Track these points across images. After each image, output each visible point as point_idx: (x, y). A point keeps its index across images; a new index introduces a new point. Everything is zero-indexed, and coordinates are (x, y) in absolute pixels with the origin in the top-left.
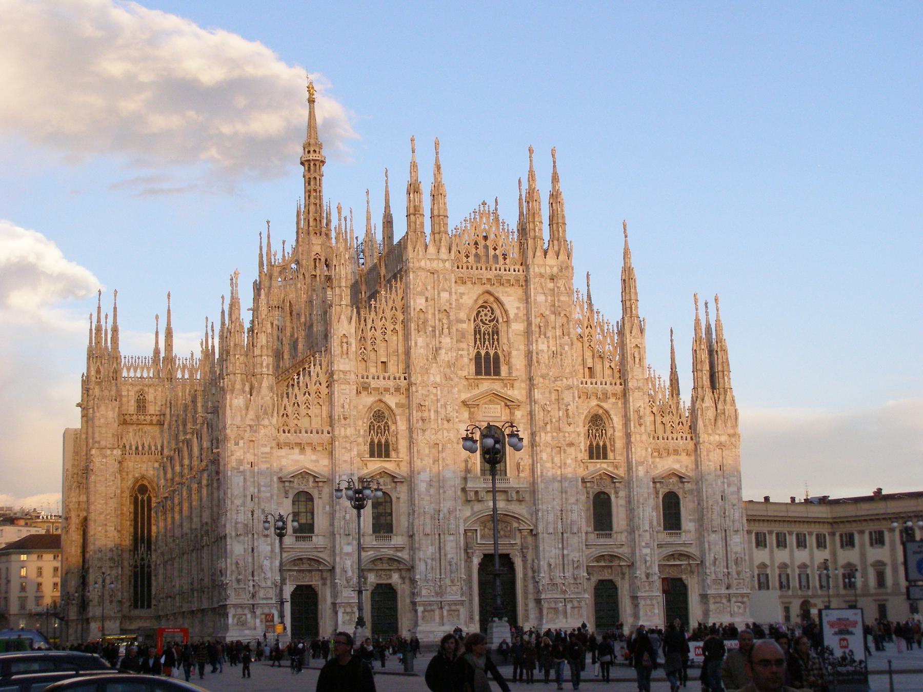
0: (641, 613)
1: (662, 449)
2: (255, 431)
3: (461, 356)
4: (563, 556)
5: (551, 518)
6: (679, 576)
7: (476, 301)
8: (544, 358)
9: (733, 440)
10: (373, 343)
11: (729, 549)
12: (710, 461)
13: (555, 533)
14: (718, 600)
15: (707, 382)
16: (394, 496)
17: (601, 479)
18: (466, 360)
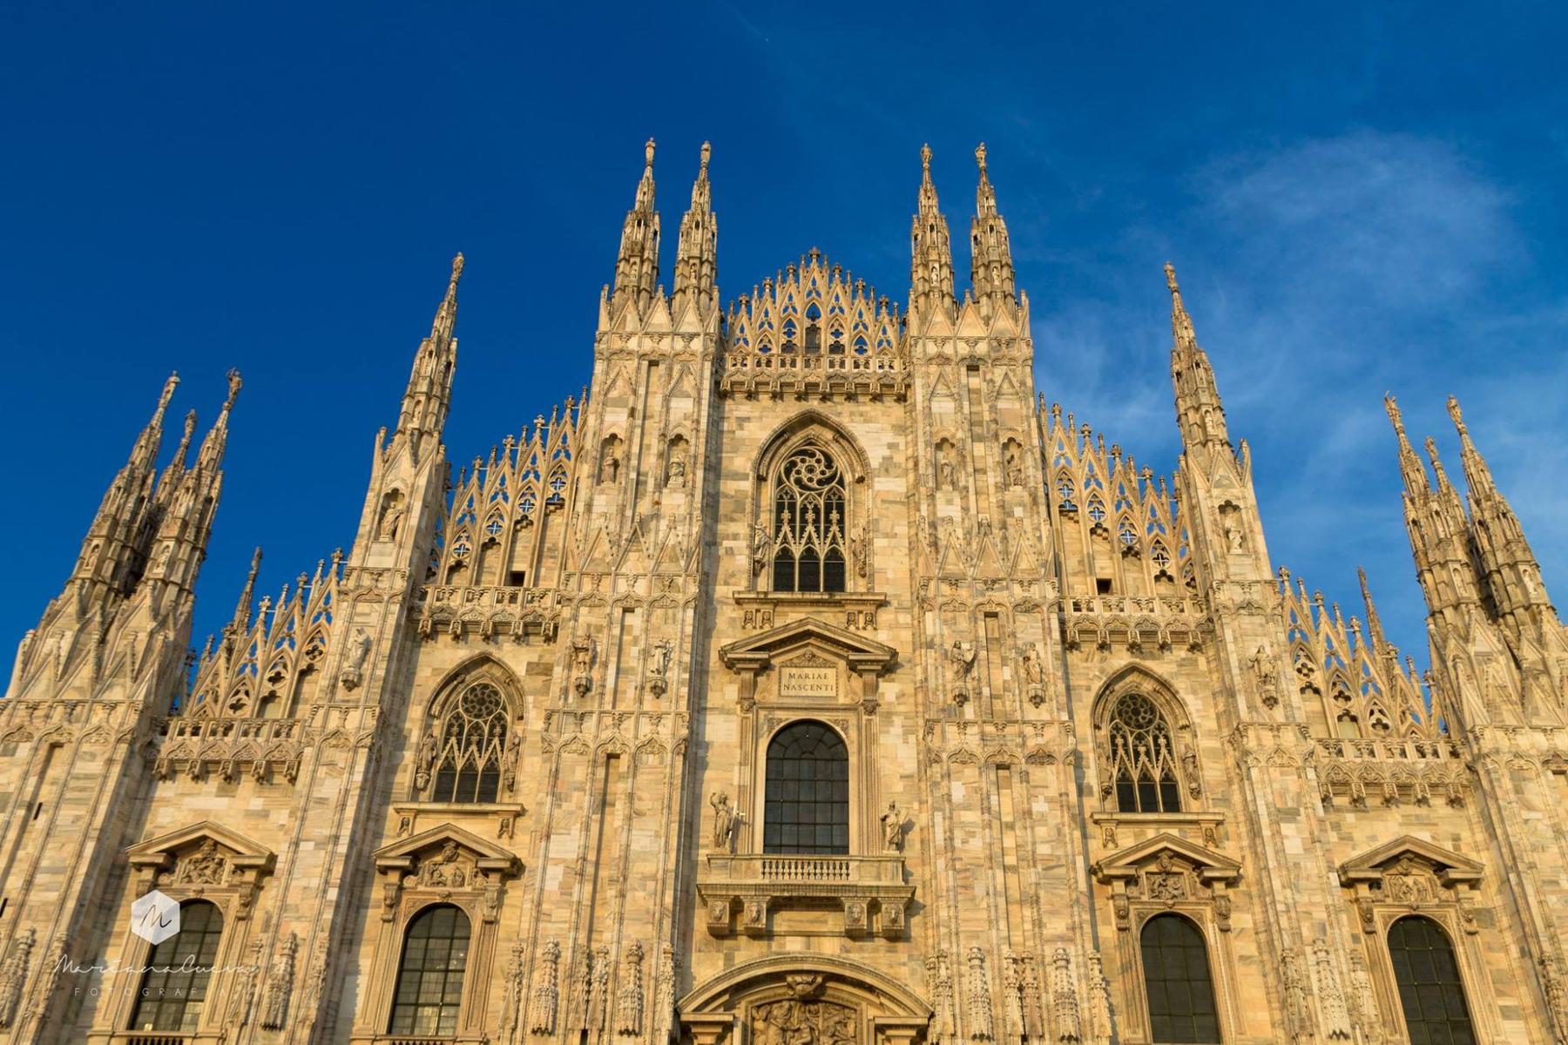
1: (1356, 787)
2: (78, 721)
3: (730, 552)
7: (781, 436)
15: (1472, 594)
16: (478, 915)
18: (743, 561)
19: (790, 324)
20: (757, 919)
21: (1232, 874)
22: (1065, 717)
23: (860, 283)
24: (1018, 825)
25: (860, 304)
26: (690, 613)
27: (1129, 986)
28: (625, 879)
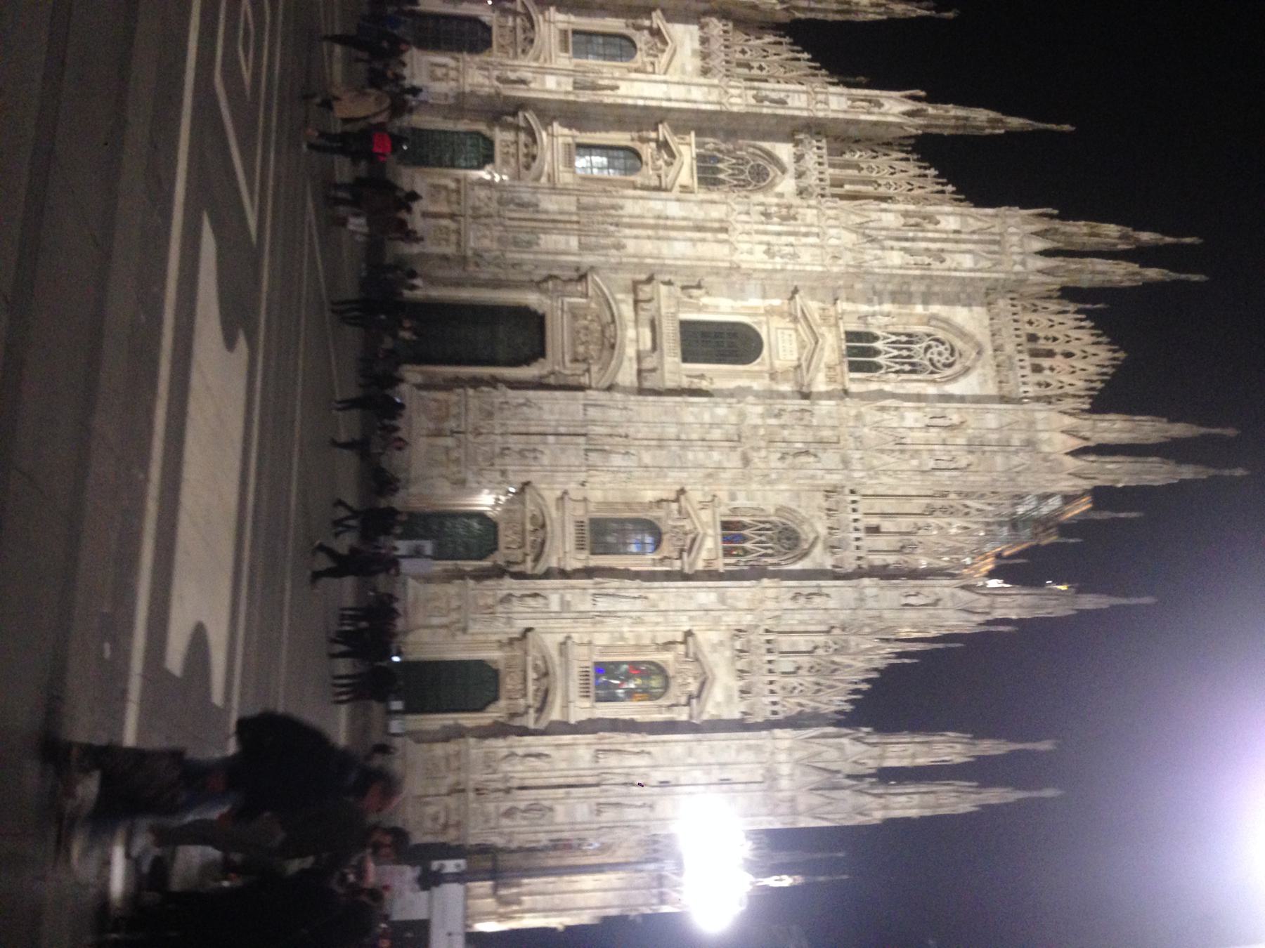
0: (434, 588)
4: (545, 434)
5: (615, 415)
6: (503, 693)
7: (962, 334)
8: (890, 419)
9: (784, 808)
10: (870, 169)
11: (562, 791)
12: (739, 751)
13: (586, 423)
14: (454, 764)
16: (638, 179)
17: (686, 534)
18: (864, 308)
19: (1055, 339)
20: (643, 310)
21: (687, 570)
22: (774, 476)
23: (1099, 385)
24: (705, 443)
25: (1081, 384)
26: (820, 269)
27: (619, 507)
28: (659, 239)
